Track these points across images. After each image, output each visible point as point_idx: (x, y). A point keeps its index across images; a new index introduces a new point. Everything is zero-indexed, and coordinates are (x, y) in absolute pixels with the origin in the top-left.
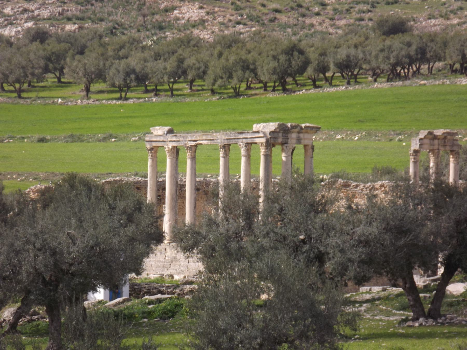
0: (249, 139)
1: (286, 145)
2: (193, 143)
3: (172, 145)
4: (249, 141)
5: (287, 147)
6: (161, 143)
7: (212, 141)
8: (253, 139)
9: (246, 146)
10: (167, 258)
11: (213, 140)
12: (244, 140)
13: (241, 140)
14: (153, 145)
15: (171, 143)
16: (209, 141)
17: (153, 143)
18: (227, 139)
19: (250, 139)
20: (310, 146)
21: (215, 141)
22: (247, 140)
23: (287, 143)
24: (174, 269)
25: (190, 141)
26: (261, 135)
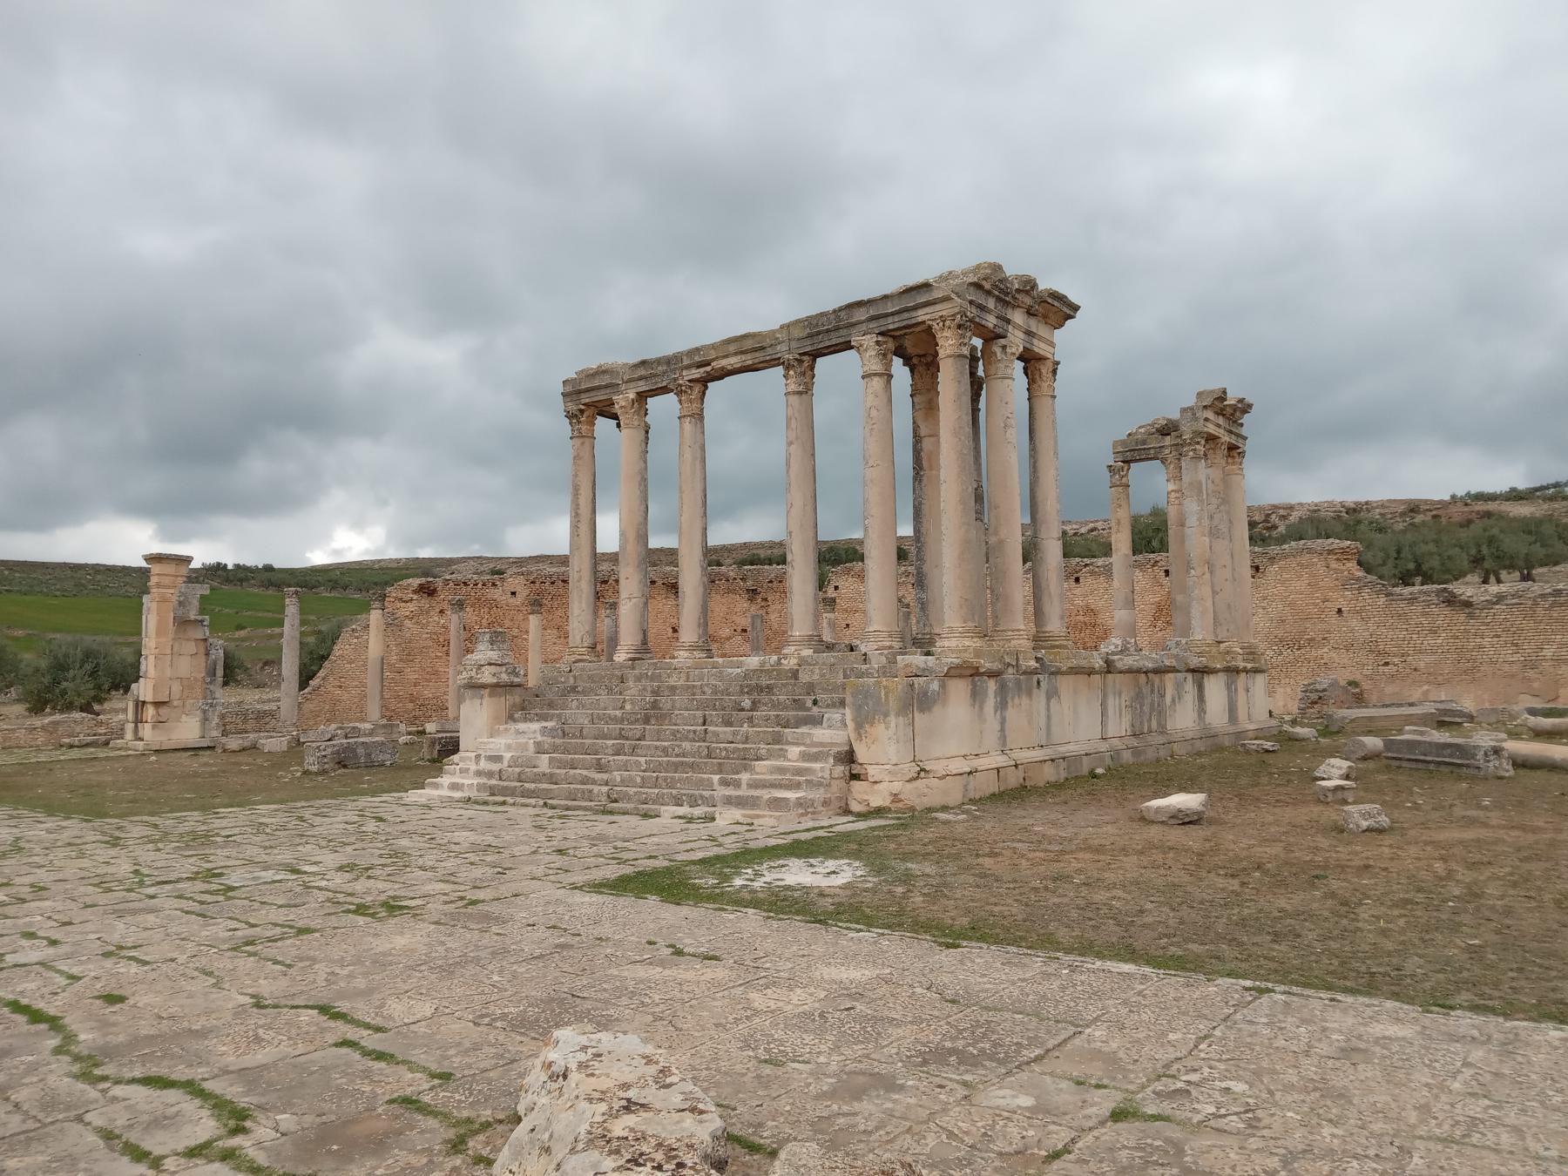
0: (890, 320)
1: (1002, 341)
2: (696, 373)
3: (635, 390)
4: (892, 324)
5: (1004, 347)
6: (603, 392)
7: (757, 354)
8: (906, 315)
9: (878, 343)
10: (628, 707)
11: (763, 348)
12: (873, 325)
13: (864, 327)
14: (583, 401)
15: (632, 385)
16: (749, 356)
17: (583, 396)
18: (810, 336)
19: (896, 318)
20: (1049, 365)
21: (770, 351)
22: (882, 321)
23: (1004, 337)
24: (656, 748)
25: (688, 367)
26: (937, 294)
